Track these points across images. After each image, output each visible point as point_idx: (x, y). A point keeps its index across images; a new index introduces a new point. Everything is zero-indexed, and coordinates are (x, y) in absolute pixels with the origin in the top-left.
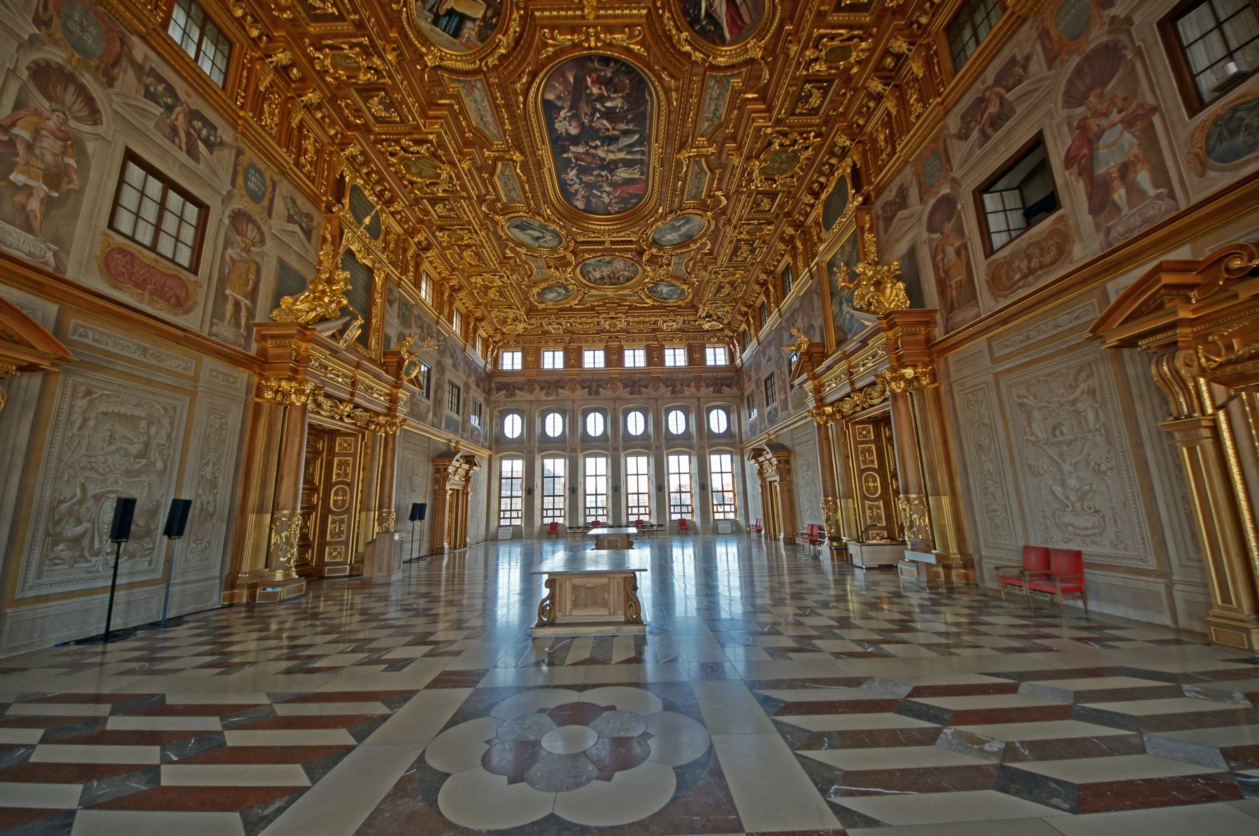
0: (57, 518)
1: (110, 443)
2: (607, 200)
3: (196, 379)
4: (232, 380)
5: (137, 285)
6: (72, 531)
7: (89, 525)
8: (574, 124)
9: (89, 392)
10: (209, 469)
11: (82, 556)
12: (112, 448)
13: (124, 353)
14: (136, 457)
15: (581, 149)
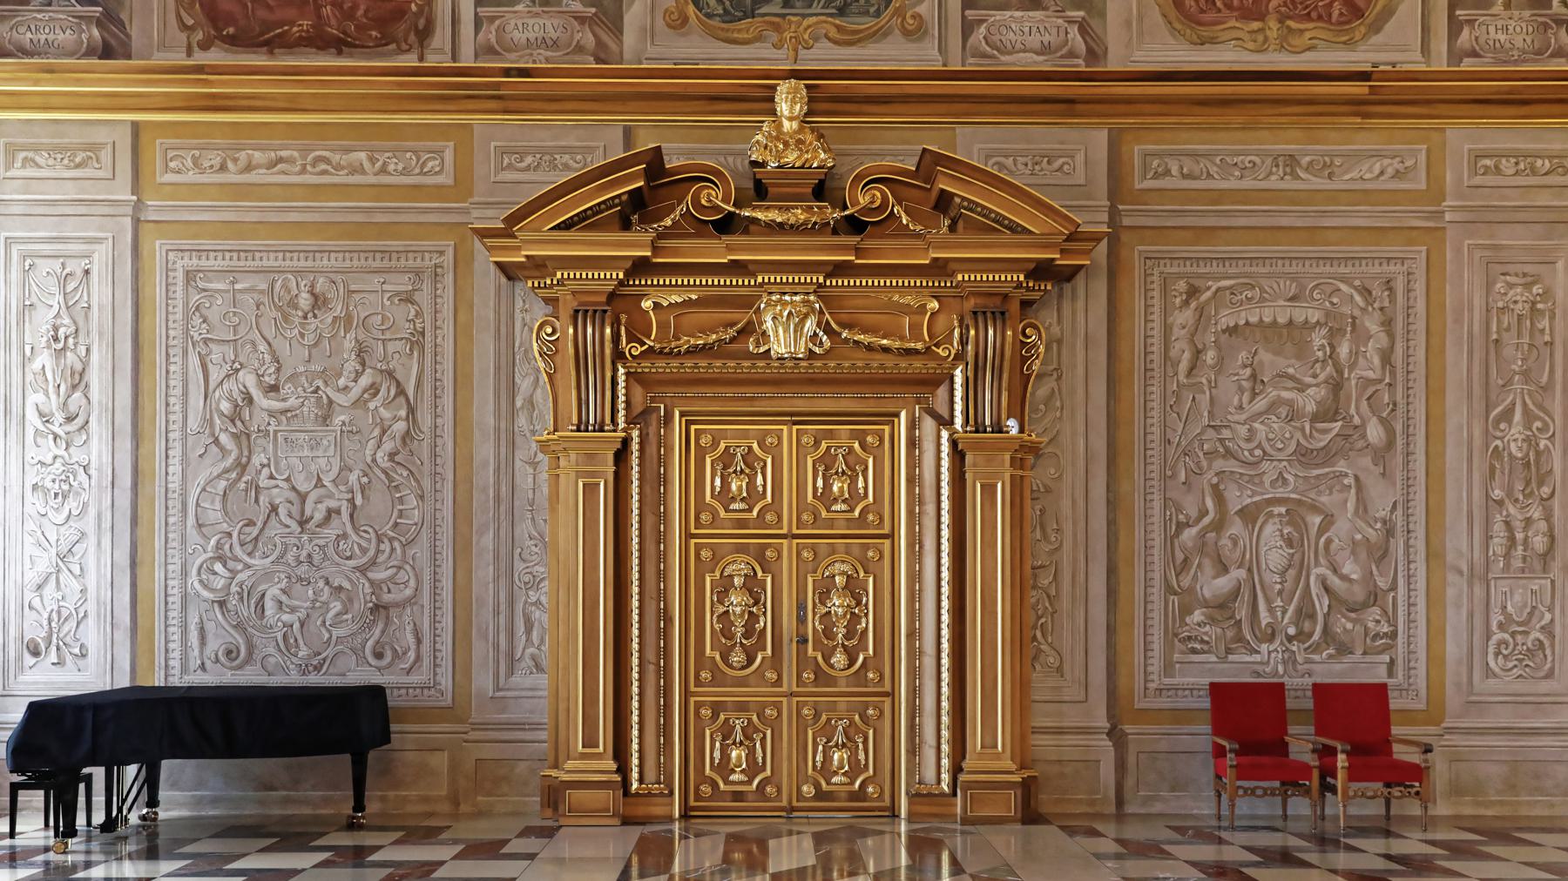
0: (1180, 556)
1: (1254, 395)
3: (1435, 192)
4: (1543, 165)
5: (1247, 14)
6: (1215, 586)
7: (1242, 574)
9: (1193, 292)
10: (1516, 430)
11: (1240, 638)
12: (1261, 404)
13: (1247, 184)
14: (1315, 418)
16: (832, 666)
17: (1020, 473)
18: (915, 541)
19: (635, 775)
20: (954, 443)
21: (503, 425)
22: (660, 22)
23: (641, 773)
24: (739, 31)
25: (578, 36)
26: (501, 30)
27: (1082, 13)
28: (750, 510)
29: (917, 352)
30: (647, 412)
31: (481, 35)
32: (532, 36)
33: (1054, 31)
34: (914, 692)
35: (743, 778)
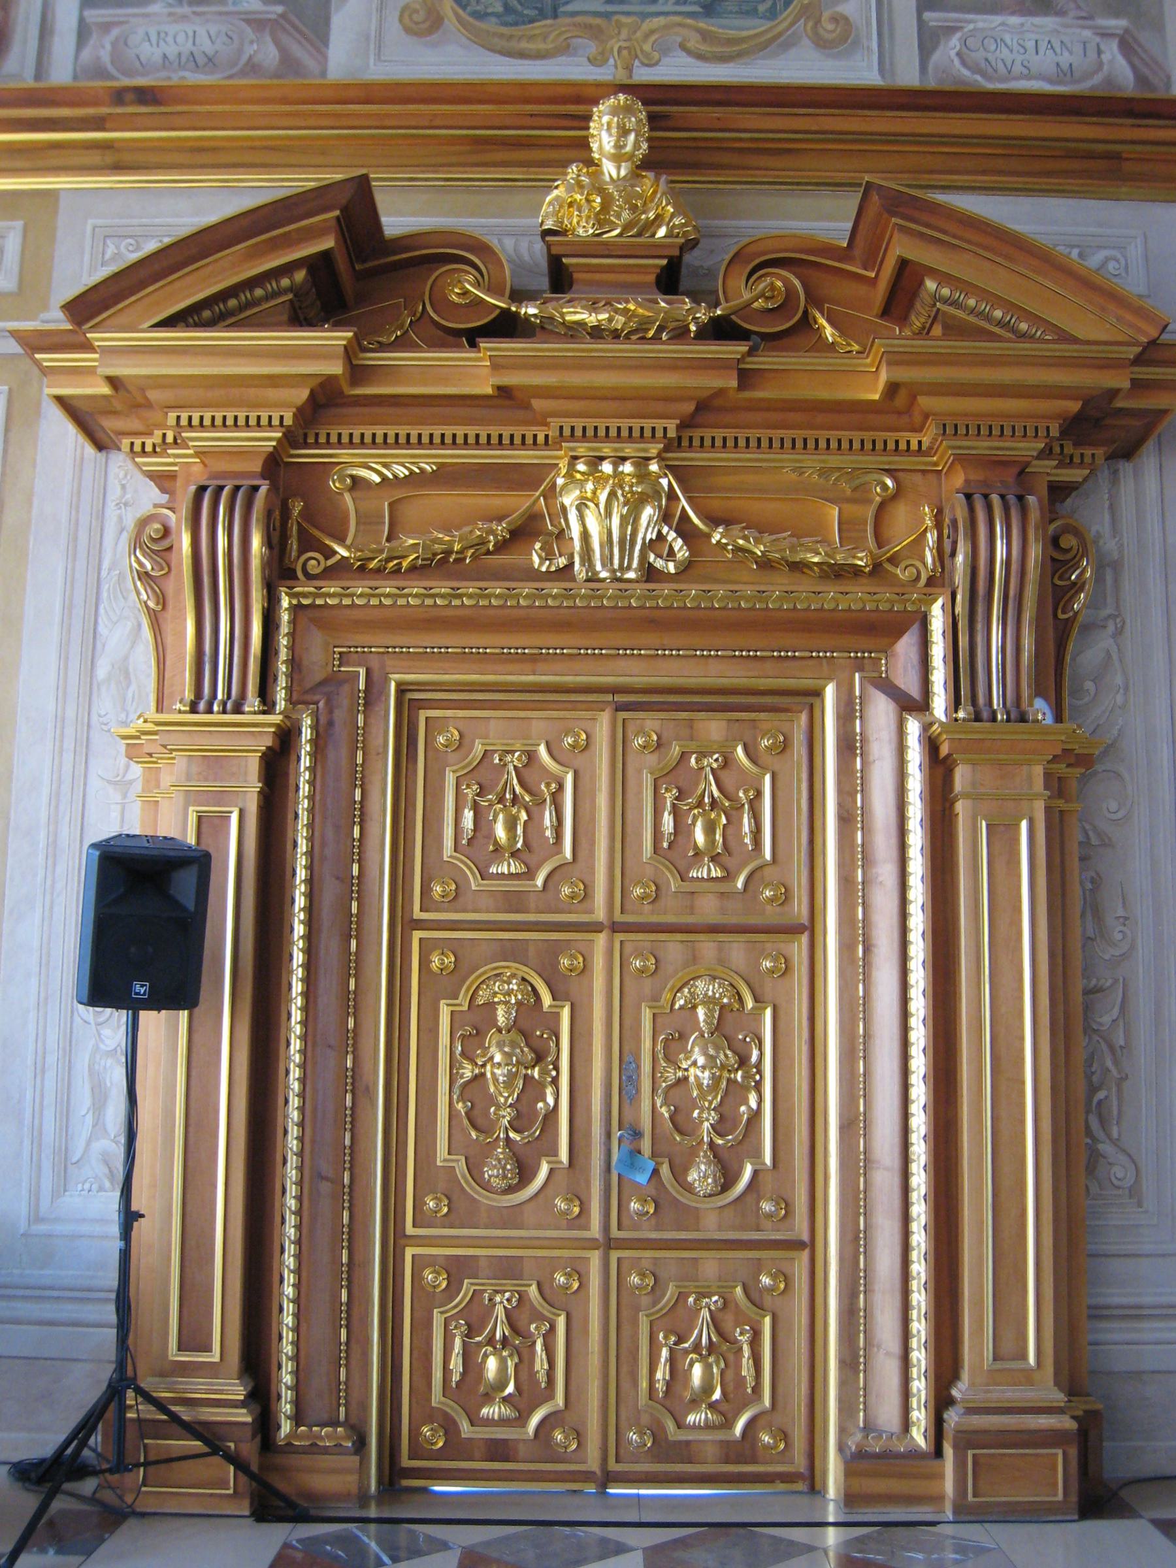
16: (689, 1188)
17: (1060, 803)
18: (857, 937)
19: (286, 1408)
20: (931, 746)
21: (71, 713)
22: (393, 28)
23: (297, 1403)
24: (531, 38)
25: (250, 50)
26: (121, 43)
27: (1123, 23)
28: (530, 874)
29: (856, 571)
30: (333, 682)
31: (86, 54)
32: (171, 50)
33: (1078, 49)
34: (856, 1241)
35: (506, 1411)
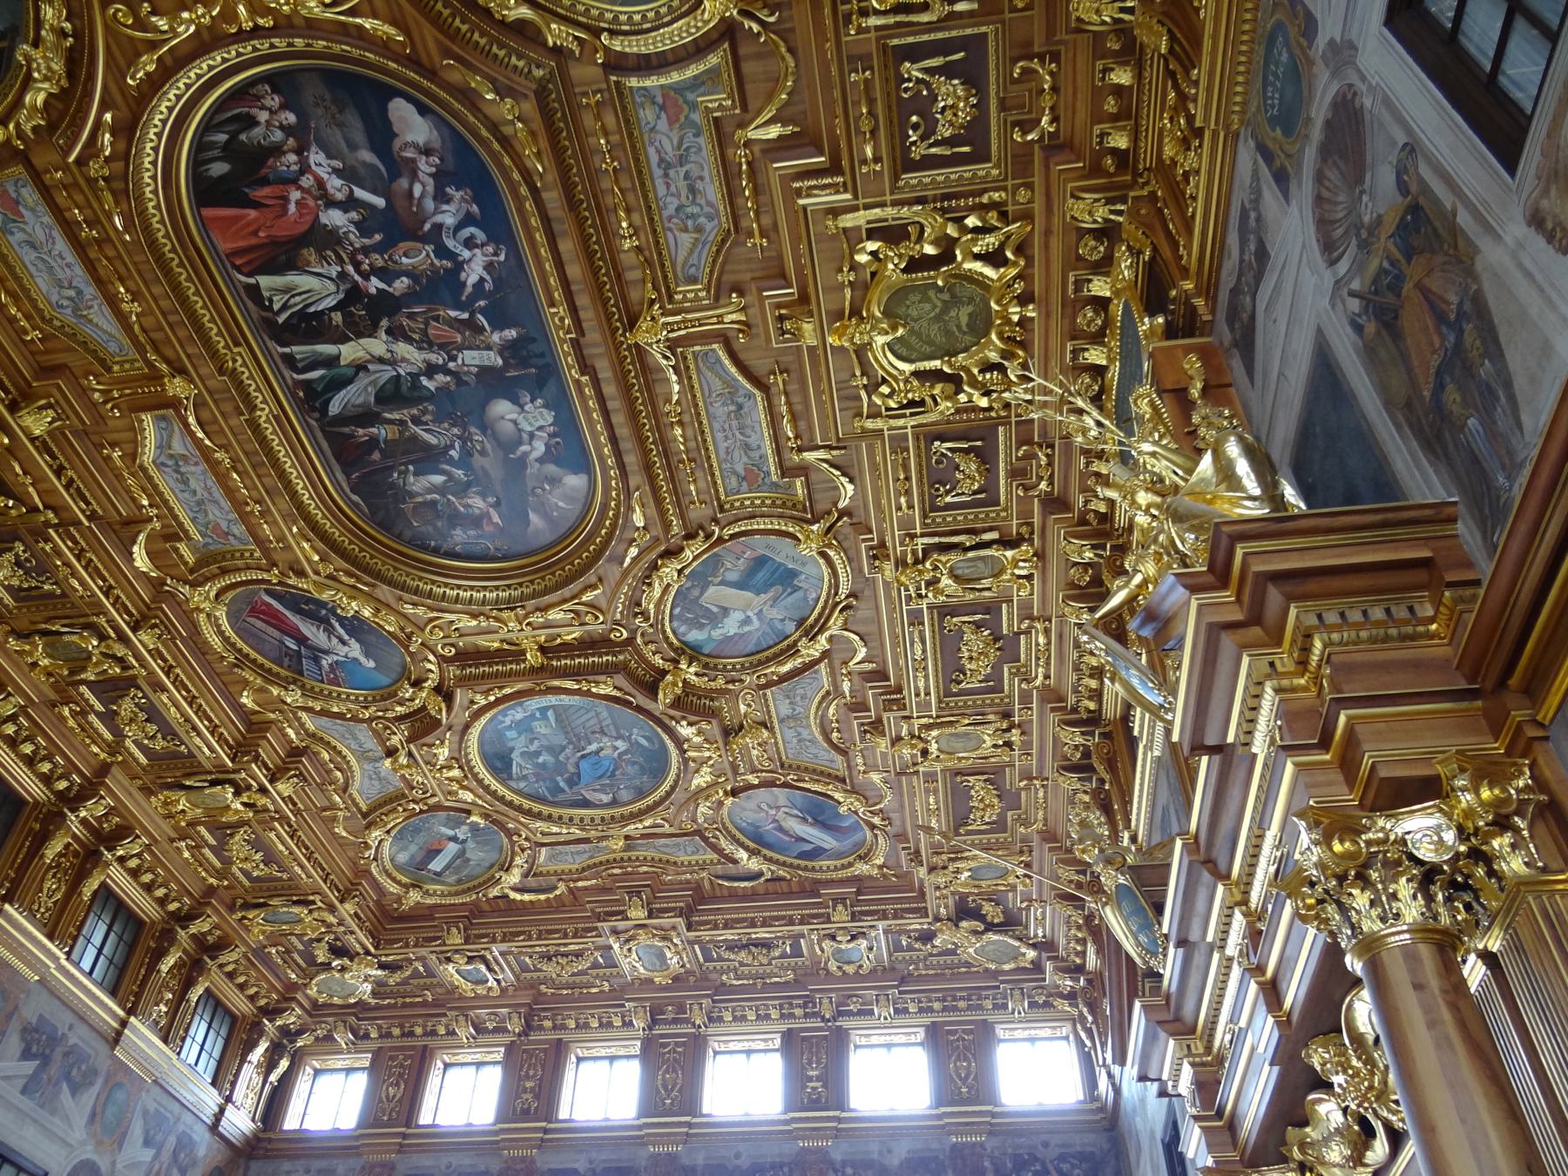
2: (316, 157)
8: (506, 428)
15: (471, 359)
